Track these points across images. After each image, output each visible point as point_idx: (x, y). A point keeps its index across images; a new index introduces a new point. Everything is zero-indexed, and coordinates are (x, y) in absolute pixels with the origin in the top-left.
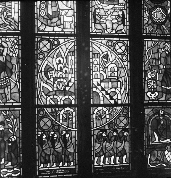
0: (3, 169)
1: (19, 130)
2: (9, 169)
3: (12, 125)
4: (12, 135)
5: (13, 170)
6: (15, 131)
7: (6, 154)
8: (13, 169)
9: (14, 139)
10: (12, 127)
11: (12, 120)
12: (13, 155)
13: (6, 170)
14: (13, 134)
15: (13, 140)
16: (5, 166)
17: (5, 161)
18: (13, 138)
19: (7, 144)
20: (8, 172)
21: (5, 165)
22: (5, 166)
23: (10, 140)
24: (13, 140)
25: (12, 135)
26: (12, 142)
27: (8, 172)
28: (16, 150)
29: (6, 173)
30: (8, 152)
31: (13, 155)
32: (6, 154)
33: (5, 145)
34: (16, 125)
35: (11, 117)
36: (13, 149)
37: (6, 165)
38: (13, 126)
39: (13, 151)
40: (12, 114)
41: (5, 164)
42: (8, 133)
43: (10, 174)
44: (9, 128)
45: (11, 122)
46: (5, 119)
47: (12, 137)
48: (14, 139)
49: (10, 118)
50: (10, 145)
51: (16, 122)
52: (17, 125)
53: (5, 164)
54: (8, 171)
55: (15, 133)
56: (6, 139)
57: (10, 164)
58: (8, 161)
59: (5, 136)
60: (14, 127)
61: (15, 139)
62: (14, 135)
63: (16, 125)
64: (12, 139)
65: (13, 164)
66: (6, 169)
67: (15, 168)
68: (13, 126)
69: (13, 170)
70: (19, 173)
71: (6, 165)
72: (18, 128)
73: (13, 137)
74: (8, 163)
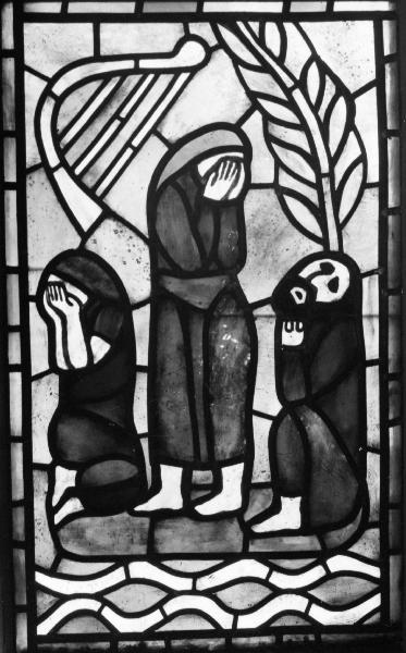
0: (229, 558)
1: (371, 199)
2: (286, 564)
3: (312, 159)
4: (318, 248)
5: (317, 573)
6: (343, 215)
7: (261, 428)
8: (320, 557)
9: (333, 285)
10: (311, 176)
11: (315, 109)
12: (316, 428)
13: (259, 570)
14: (324, 241)
15: (324, 296)
16: (249, 536)
17: (248, 486)
18: (320, 282)
19: (265, 332)
20: (277, 592)
21: (246, 528)
22: (249, 536)
23: (298, 295)
24: (324, 296)
25: (318, 248)
26: (314, 317)
27: (277, 592)
28: (349, 389)
29: (257, 598)
30: (275, 408)
31: (316, 428)
32: (261, 428)
33: (252, 344)
34: (352, 152)
35: (301, 84)
36: (325, 370)
37: (260, 528)
38: (325, 167)
39: (319, 400)
40: (315, 58)
41: (248, 516)
42: (279, 237)
43: (299, 603)
44: (286, 181)
45: (303, 126)
46: (253, 96)
47: (315, 266)
48: (333, 285)
49: (297, 95)
50: (293, 338)
51: (350, 126)
52: (362, 159)
53: (248, 516)
54: (279, 580)
55: (340, 227)
56: (257, 284)
57: (290, 513)
58: (280, 487)
59: (250, 259)
60: (331, 175)
61: (344, 285)
62: (334, 246)
63: (352, 152)
64: (312, 291)
65: (319, 519)
66: (262, 558)
67: (343, 549)
68: (325, 167)
69: (317, 573)
70: (375, 602)
71: (260, 528)
72: (365, 185)
73: (327, 269)
74: (275, 509)
